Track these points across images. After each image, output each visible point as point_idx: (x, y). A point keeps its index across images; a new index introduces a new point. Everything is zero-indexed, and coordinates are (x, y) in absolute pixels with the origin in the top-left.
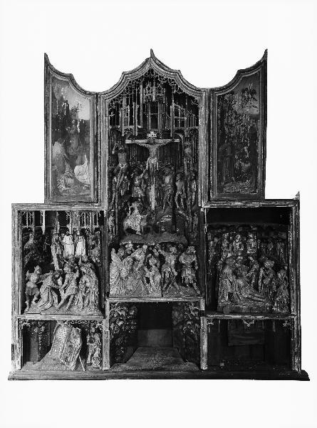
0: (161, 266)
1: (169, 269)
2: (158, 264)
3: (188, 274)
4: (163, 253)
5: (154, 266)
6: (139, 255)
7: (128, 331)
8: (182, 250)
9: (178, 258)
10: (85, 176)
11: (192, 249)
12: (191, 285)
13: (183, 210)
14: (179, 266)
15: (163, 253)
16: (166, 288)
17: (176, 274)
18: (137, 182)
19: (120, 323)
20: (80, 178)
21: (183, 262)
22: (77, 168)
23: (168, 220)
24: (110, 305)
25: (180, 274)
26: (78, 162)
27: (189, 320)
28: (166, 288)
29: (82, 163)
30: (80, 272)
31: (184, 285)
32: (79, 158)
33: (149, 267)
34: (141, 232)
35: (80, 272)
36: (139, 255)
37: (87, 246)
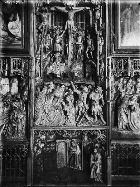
0: (75, 101)
1: (82, 105)
2: (73, 100)
3: (97, 109)
4: (79, 92)
5: (70, 102)
6: (60, 93)
7: (48, 151)
8: (94, 89)
9: (88, 95)
10: (17, 30)
11: (100, 88)
12: (99, 117)
13: (91, 59)
14: (90, 102)
15: (79, 92)
16: (80, 119)
17: (88, 108)
18: (58, 41)
19: (42, 145)
20: (12, 32)
21: (93, 98)
22: (10, 24)
23: (79, 68)
24: (35, 132)
25: (90, 107)
26: (11, 19)
27: (97, 143)
28: (80, 119)
29: (14, 20)
30: (11, 106)
31: (93, 117)
32: (12, 15)
33: (66, 103)
34: (60, 75)
35: (11, 106)
36: (60, 93)
37: (19, 86)
